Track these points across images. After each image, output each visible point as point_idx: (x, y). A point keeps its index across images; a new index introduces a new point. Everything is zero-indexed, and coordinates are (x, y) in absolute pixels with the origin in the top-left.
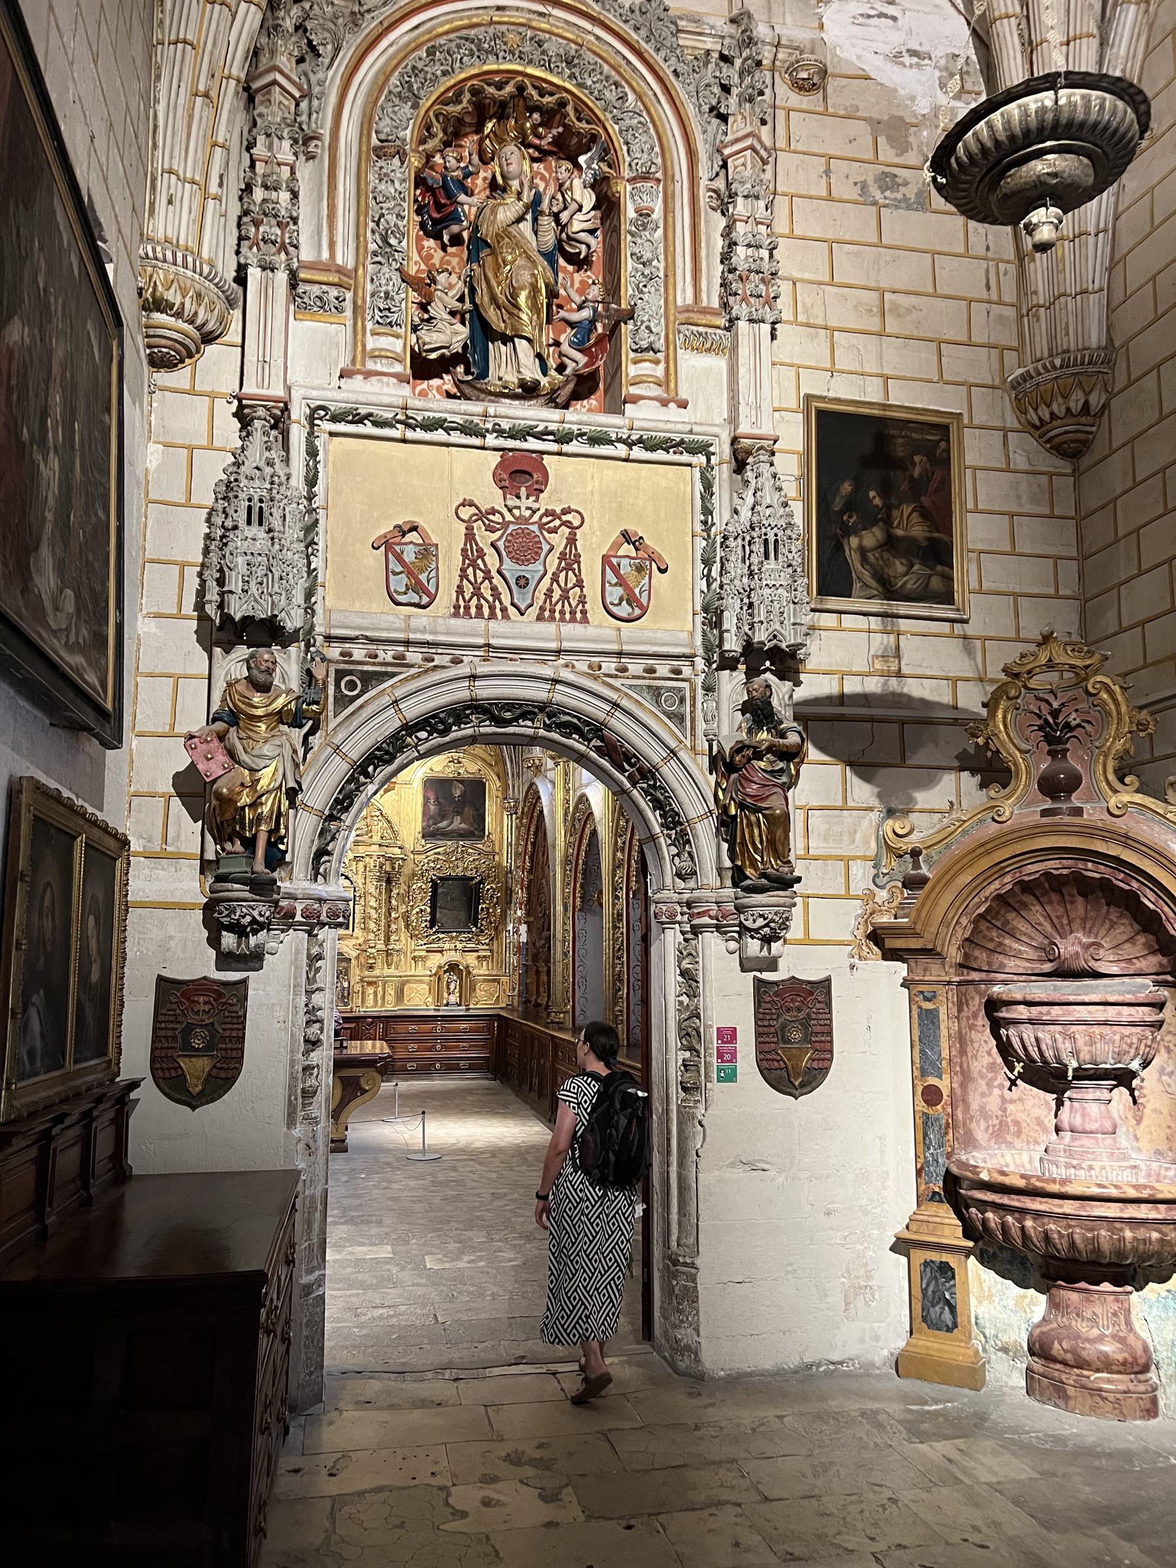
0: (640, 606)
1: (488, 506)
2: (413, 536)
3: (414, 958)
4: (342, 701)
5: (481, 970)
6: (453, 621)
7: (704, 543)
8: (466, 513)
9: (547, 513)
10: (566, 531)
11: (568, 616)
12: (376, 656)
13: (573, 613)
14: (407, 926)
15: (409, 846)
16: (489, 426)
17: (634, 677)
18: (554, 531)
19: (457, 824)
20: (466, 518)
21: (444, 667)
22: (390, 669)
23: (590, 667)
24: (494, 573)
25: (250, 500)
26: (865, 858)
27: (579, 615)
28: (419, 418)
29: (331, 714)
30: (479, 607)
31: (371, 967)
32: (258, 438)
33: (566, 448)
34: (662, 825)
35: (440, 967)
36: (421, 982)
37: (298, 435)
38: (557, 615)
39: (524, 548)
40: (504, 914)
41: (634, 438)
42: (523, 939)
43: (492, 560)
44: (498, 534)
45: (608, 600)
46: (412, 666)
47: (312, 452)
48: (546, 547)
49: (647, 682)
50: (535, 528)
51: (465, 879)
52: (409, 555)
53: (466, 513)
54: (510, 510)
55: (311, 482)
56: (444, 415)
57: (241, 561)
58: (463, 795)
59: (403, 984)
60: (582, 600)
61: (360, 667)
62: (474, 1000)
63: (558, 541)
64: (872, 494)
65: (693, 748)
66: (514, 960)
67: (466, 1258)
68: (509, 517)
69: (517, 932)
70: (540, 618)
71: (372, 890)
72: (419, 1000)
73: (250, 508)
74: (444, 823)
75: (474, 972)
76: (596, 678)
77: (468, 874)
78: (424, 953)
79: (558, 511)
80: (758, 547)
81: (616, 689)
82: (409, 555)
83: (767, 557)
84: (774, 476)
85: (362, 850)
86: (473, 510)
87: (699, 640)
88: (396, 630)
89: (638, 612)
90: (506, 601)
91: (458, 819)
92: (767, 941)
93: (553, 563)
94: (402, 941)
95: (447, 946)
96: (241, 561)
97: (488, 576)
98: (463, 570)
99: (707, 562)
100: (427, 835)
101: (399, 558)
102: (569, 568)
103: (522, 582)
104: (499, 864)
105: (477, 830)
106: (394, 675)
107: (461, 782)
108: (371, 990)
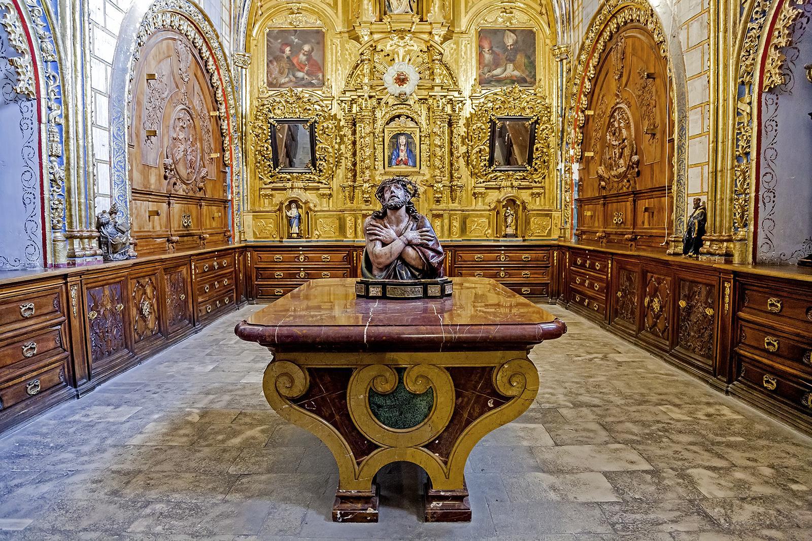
19: (511, 71)
31: (438, 201)
36: (482, 216)
42: (576, 177)
58: (516, 42)
69: (569, 170)
72: (481, 231)
74: (498, 71)
75: (529, 208)
91: (510, 66)
105: (528, 79)
107: (513, 31)
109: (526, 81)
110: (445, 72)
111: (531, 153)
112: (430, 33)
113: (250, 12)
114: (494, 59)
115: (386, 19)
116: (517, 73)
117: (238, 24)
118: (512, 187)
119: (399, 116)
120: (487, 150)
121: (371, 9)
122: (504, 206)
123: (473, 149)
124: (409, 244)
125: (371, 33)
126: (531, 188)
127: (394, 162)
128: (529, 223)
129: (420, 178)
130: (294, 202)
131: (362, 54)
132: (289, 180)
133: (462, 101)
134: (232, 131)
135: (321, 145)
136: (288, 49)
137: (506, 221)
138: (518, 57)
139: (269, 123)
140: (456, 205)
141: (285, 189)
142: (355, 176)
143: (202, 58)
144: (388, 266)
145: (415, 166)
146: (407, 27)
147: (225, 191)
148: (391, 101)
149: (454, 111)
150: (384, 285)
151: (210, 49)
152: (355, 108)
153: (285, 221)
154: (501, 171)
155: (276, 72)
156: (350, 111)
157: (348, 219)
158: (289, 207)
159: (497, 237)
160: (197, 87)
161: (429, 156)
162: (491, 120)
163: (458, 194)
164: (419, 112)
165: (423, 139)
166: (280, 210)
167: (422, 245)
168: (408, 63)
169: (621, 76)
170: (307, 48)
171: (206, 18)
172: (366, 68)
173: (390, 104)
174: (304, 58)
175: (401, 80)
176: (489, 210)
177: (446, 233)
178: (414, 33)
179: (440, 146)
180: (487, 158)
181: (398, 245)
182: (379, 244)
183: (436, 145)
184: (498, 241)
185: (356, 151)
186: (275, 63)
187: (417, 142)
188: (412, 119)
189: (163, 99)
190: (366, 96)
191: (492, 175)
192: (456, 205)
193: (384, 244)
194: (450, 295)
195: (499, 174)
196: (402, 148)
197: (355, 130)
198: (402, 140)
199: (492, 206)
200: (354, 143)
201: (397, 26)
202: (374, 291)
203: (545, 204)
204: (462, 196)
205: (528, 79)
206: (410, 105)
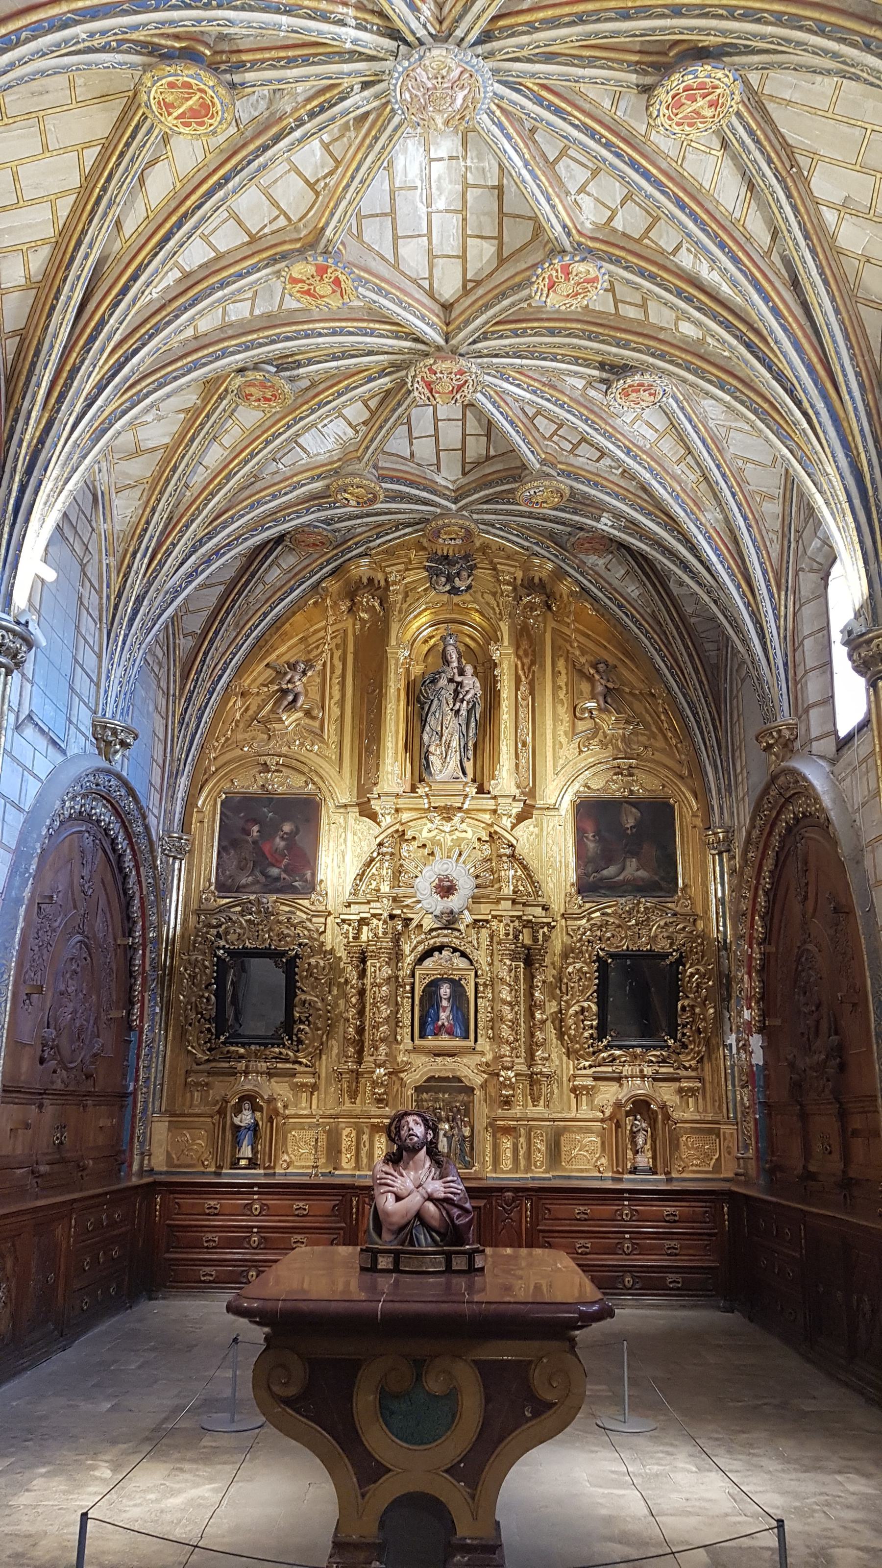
3: (574, 1090)
5: (686, 1112)
14: (561, 1035)
19: (632, 870)
31: (507, 1102)
35: (618, 1105)
36: (589, 1130)
40: (719, 1018)
42: (758, 1058)
58: (638, 825)
62: (677, 1165)
66: (744, 1096)
71: (504, 974)
72: (587, 1161)
75: (676, 1115)
78: (589, 1082)
94: (554, 1058)
95: (627, 1070)
100: (588, 887)
104: (704, 936)
105: (662, 882)
107: (634, 805)
108: (507, 1144)
109: (661, 889)
110: (519, 872)
112: (495, 811)
113: (195, 768)
116: (641, 873)
117: (173, 787)
118: (643, 1077)
119: (440, 949)
120: (594, 1008)
122: (628, 1114)
123: (569, 1006)
124: (430, 1198)
125: (397, 810)
126: (678, 1080)
127: (430, 1028)
128: (678, 1146)
129: (472, 1060)
130: (250, 1099)
131: (380, 844)
132: (242, 1057)
133: (548, 924)
134: (147, 968)
135: (303, 997)
136: (256, 828)
137: (634, 1143)
138: (645, 846)
139: (216, 955)
140: (540, 1108)
141: (235, 1074)
142: (360, 1052)
143: (114, 850)
144: (402, 1228)
145: (467, 1037)
146: (456, 802)
147: (124, 1076)
148: (428, 923)
149: (535, 939)
150: (397, 1254)
151: (128, 836)
153: (229, 1134)
154: (620, 1047)
155: (232, 866)
156: (356, 938)
157: (345, 1133)
158: (238, 1110)
159: (618, 1172)
160: (103, 902)
161: (492, 1020)
162: (599, 959)
163: (544, 1090)
164: (475, 942)
165: (481, 988)
166: (222, 1112)
167: (446, 1200)
168: (457, 861)
169: (806, 898)
170: (287, 828)
171: (131, 792)
172: (386, 871)
174: (282, 844)
175: (446, 889)
176: (602, 1121)
177: (523, 1162)
178: (468, 811)
179: (510, 1004)
180: (595, 1023)
181: (414, 1201)
182: (391, 1198)
183: (504, 1002)
184: (621, 1180)
185: (364, 1007)
186: (232, 852)
187: (471, 994)
188: (464, 955)
189: (54, 930)
190: (386, 914)
191: (605, 1055)
192: (540, 1110)
193: (398, 1198)
194: (482, 1269)
195: (618, 1053)
196: (445, 1003)
197: (364, 971)
198: (445, 990)
199: (608, 1113)
200: (362, 993)
202: (384, 1262)
203: (705, 1111)
204: (552, 1093)
205: (663, 884)
206: (459, 930)
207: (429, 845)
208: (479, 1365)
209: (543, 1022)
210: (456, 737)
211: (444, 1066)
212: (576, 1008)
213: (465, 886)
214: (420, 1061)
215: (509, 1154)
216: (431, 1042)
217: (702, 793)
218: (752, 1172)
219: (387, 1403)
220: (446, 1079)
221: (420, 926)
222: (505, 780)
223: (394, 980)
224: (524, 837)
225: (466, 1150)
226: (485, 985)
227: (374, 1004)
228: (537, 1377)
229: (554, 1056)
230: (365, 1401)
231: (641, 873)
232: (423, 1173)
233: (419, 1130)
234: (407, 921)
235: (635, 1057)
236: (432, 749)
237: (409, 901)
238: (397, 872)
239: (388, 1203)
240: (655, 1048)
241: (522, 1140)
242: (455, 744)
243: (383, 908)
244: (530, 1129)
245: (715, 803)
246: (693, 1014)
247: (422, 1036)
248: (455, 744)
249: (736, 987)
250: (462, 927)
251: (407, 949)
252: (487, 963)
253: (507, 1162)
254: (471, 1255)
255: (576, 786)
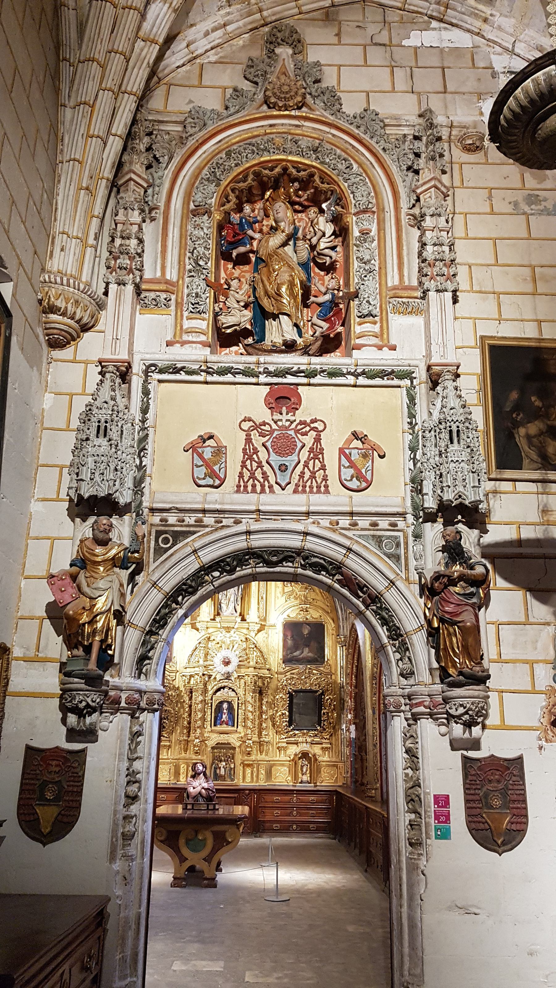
0: (366, 480)
1: (261, 421)
2: (211, 442)
3: (278, 748)
4: (159, 552)
5: (324, 758)
6: (236, 495)
7: (411, 437)
8: (246, 425)
9: (301, 423)
10: (313, 434)
11: (315, 490)
12: (183, 521)
13: (319, 487)
14: (273, 725)
15: (274, 668)
16: (261, 370)
17: (362, 529)
18: (306, 434)
19: (306, 653)
20: (246, 429)
21: (229, 526)
22: (192, 529)
23: (331, 523)
24: (264, 463)
25: (99, 422)
26: (546, 662)
27: (323, 489)
28: (215, 368)
29: (151, 560)
30: (254, 486)
31: (249, 754)
32: (108, 383)
33: (312, 381)
34: (388, 637)
35: (296, 755)
36: (283, 765)
37: (136, 382)
38: (308, 489)
39: (284, 446)
40: (339, 717)
41: (359, 371)
42: (353, 735)
43: (263, 455)
44: (268, 437)
45: (343, 478)
46: (207, 526)
47: (146, 393)
48: (299, 445)
49: (372, 533)
50: (292, 433)
51: (311, 691)
52: (208, 454)
53: (246, 425)
54: (276, 422)
55: (145, 410)
56: (231, 365)
57: (90, 460)
59: (271, 766)
60: (325, 479)
61: (172, 529)
63: (309, 440)
64: (533, 399)
65: (407, 579)
66: (347, 751)
67: (276, 975)
68: (274, 426)
69: (348, 730)
70: (295, 491)
71: (249, 699)
72: (282, 778)
73: (99, 426)
74: (297, 653)
75: (320, 759)
76: (334, 531)
77: (314, 688)
78: (285, 745)
79: (308, 421)
80: (445, 436)
81: (350, 538)
82: (208, 454)
83: (452, 442)
84: (456, 389)
85: (243, 671)
86: (251, 423)
87: (409, 503)
88: (196, 503)
89: (364, 485)
90: (272, 481)
91: (306, 650)
92: (469, 725)
93: (304, 455)
94: (270, 735)
95: (300, 739)
96: (90, 460)
97: (260, 465)
98: (244, 462)
99: (413, 450)
100: (286, 661)
101: (201, 456)
102: (315, 458)
103: (283, 468)
104: (335, 682)
105: (319, 658)
106: (194, 533)
107: (308, 624)
108: (248, 771)
109: (317, 661)
111: (320, 716)
114: (294, 644)
115: (218, 619)
116: (310, 654)
119: (224, 688)
120: (287, 713)
121: (207, 611)
122: (300, 758)
124: (203, 788)
126: (321, 744)
131: (200, 643)
133: (269, 677)
135: (166, 708)
137: (302, 771)
140: (263, 756)
145: (234, 726)
148: (219, 677)
149: (264, 684)
150: (193, 804)
152: (192, 681)
154: (298, 730)
157: (182, 766)
161: (244, 719)
162: (289, 693)
163: (265, 747)
173: (218, 679)
177: (255, 779)
178: (237, 629)
181: (199, 789)
183: (249, 711)
187: (236, 707)
188: (233, 690)
190: (201, 674)
192: (263, 757)
193: (194, 788)
195: (297, 732)
196: (225, 711)
197: (192, 696)
198: (225, 706)
199: (292, 758)
200: (190, 706)
201: (226, 625)
202: (189, 807)
204: (269, 749)
207: (220, 643)
208: (212, 832)
209: (266, 719)
210: (233, 596)
211: (223, 738)
212: (280, 713)
213: (235, 662)
214: (213, 736)
215: (249, 775)
216: (219, 728)
217: (336, 620)
218: (349, 783)
219: (187, 842)
220: (224, 744)
221: (215, 678)
222: (253, 616)
223: (204, 701)
224: (260, 639)
225: (232, 773)
226: (242, 704)
227: (195, 712)
228: (227, 834)
229: (270, 733)
230: (182, 842)
231: (310, 654)
232: (202, 781)
233: (201, 768)
234: (210, 676)
235: (304, 734)
236: (222, 601)
237: (211, 667)
238: (206, 655)
239: (191, 790)
240: (312, 730)
241: (255, 769)
242: (232, 599)
243: (200, 671)
244: (259, 764)
245: (341, 624)
246: (328, 716)
247: (215, 725)
248: (232, 599)
249: (346, 704)
250: (233, 679)
251: (209, 688)
252: (243, 695)
253: (248, 779)
254: (214, 805)
255: (285, 616)
